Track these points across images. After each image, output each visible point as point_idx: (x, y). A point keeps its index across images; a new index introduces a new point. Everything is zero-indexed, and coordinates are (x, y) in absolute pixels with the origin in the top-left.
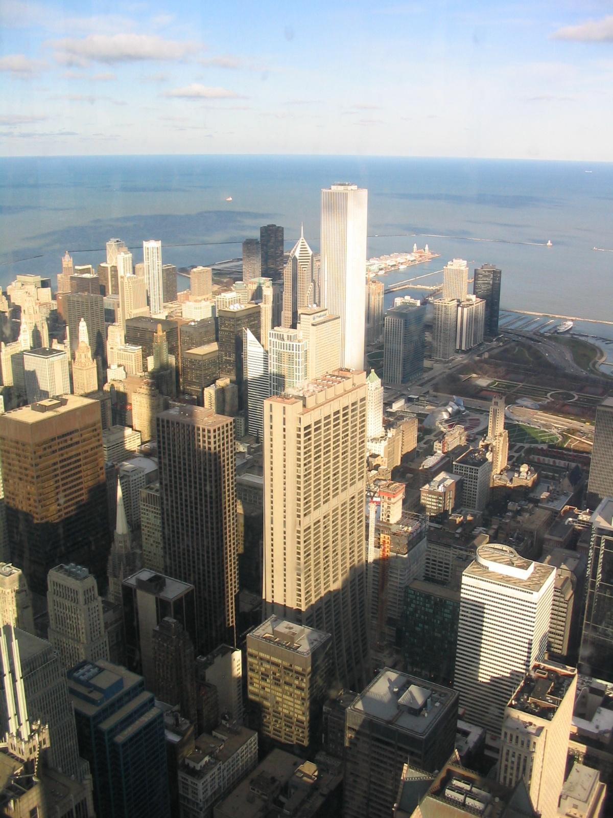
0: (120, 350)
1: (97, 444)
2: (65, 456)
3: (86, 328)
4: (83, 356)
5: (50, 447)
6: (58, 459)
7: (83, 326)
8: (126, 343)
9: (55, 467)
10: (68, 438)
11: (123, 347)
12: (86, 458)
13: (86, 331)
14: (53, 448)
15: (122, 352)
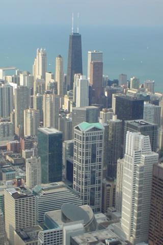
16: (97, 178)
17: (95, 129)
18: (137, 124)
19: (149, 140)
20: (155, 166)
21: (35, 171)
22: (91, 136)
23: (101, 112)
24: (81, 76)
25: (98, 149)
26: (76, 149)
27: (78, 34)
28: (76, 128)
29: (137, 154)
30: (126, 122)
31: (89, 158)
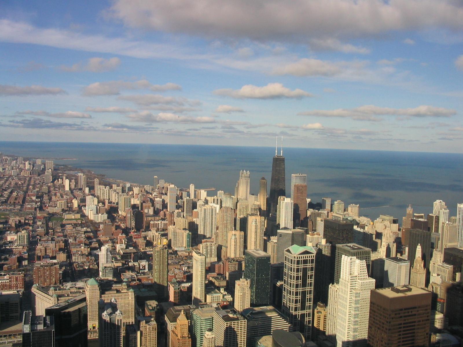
0: (439, 265)
1: (427, 318)
2: (407, 321)
3: (420, 249)
4: (418, 265)
5: (399, 314)
6: (402, 322)
7: (419, 248)
8: (443, 262)
9: (401, 326)
10: (410, 310)
11: (441, 264)
12: (418, 325)
13: (420, 251)
14: (400, 315)
15: (440, 267)
16: (307, 304)
17: (306, 252)
18: (349, 248)
19: (365, 265)
20: (372, 292)
21: (244, 294)
22: (302, 259)
23: (307, 235)
24: (285, 199)
25: (309, 273)
26: (287, 272)
27: (282, 157)
28: (286, 251)
29: (353, 278)
30: (338, 245)
31: (300, 282)
